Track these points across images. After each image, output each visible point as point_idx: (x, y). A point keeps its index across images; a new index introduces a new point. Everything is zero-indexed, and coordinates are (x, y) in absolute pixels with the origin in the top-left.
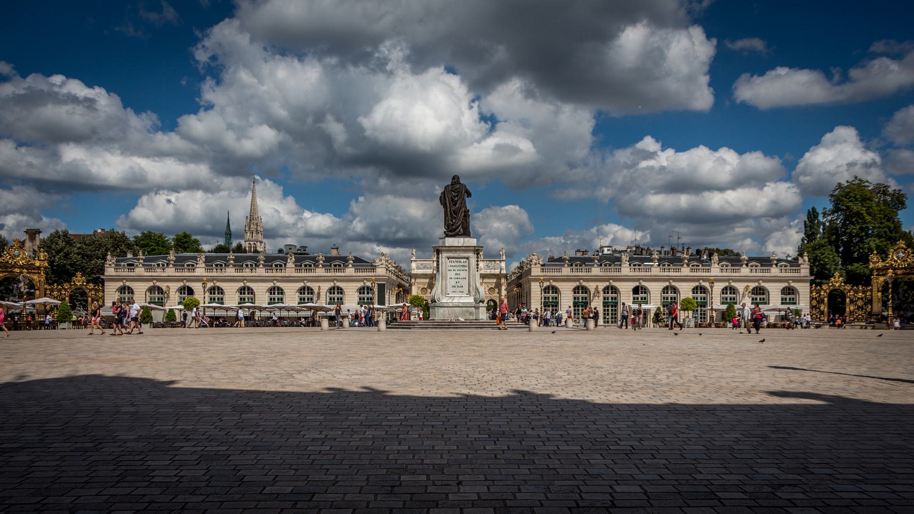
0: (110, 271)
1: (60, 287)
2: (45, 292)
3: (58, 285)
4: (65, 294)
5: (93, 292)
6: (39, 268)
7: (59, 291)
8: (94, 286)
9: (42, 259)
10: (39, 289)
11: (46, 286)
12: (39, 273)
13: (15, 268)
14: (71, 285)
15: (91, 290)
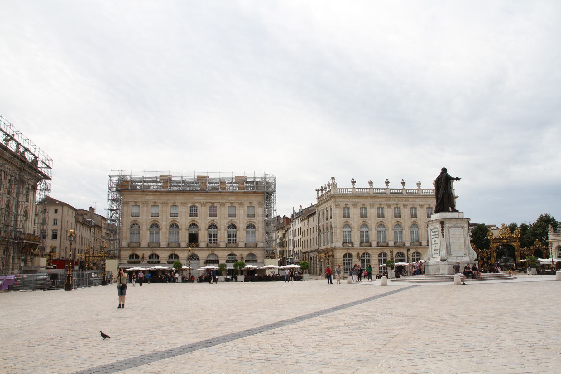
0: (551, 237)
1: (528, 249)
2: (521, 252)
3: (527, 248)
4: (531, 253)
5: (545, 251)
6: (515, 238)
7: (528, 251)
8: (546, 247)
9: (517, 233)
10: (517, 251)
11: (521, 249)
12: (516, 242)
13: (504, 240)
14: (534, 247)
15: (544, 249)
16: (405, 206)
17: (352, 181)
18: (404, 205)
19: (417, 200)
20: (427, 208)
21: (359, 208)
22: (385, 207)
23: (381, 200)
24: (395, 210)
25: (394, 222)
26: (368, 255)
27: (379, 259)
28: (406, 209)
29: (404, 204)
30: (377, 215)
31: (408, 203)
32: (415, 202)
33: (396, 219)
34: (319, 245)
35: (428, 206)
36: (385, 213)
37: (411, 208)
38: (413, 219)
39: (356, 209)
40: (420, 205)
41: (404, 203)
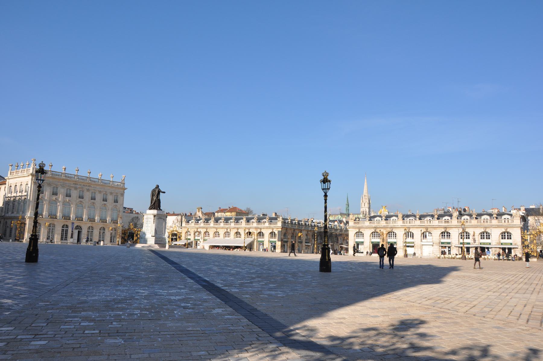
16: (88, 190)
17: (50, 164)
18: (87, 190)
19: (98, 187)
20: (104, 194)
21: (52, 187)
22: (73, 189)
23: (70, 183)
24: (80, 193)
25: (77, 201)
26: (54, 225)
27: (62, 230)
28: (88, 193)
29: (87, 189)
30: (65, 194)
31: (91, 188)
32: (96, 188)
33: (80, 199)
34: (5, 212)
35: (105, 193)
36: (71, 193)
37: (92, 192)
38: (92, 201)
39: (49, 187)
40: (99, 191)
41: (87, 188)
